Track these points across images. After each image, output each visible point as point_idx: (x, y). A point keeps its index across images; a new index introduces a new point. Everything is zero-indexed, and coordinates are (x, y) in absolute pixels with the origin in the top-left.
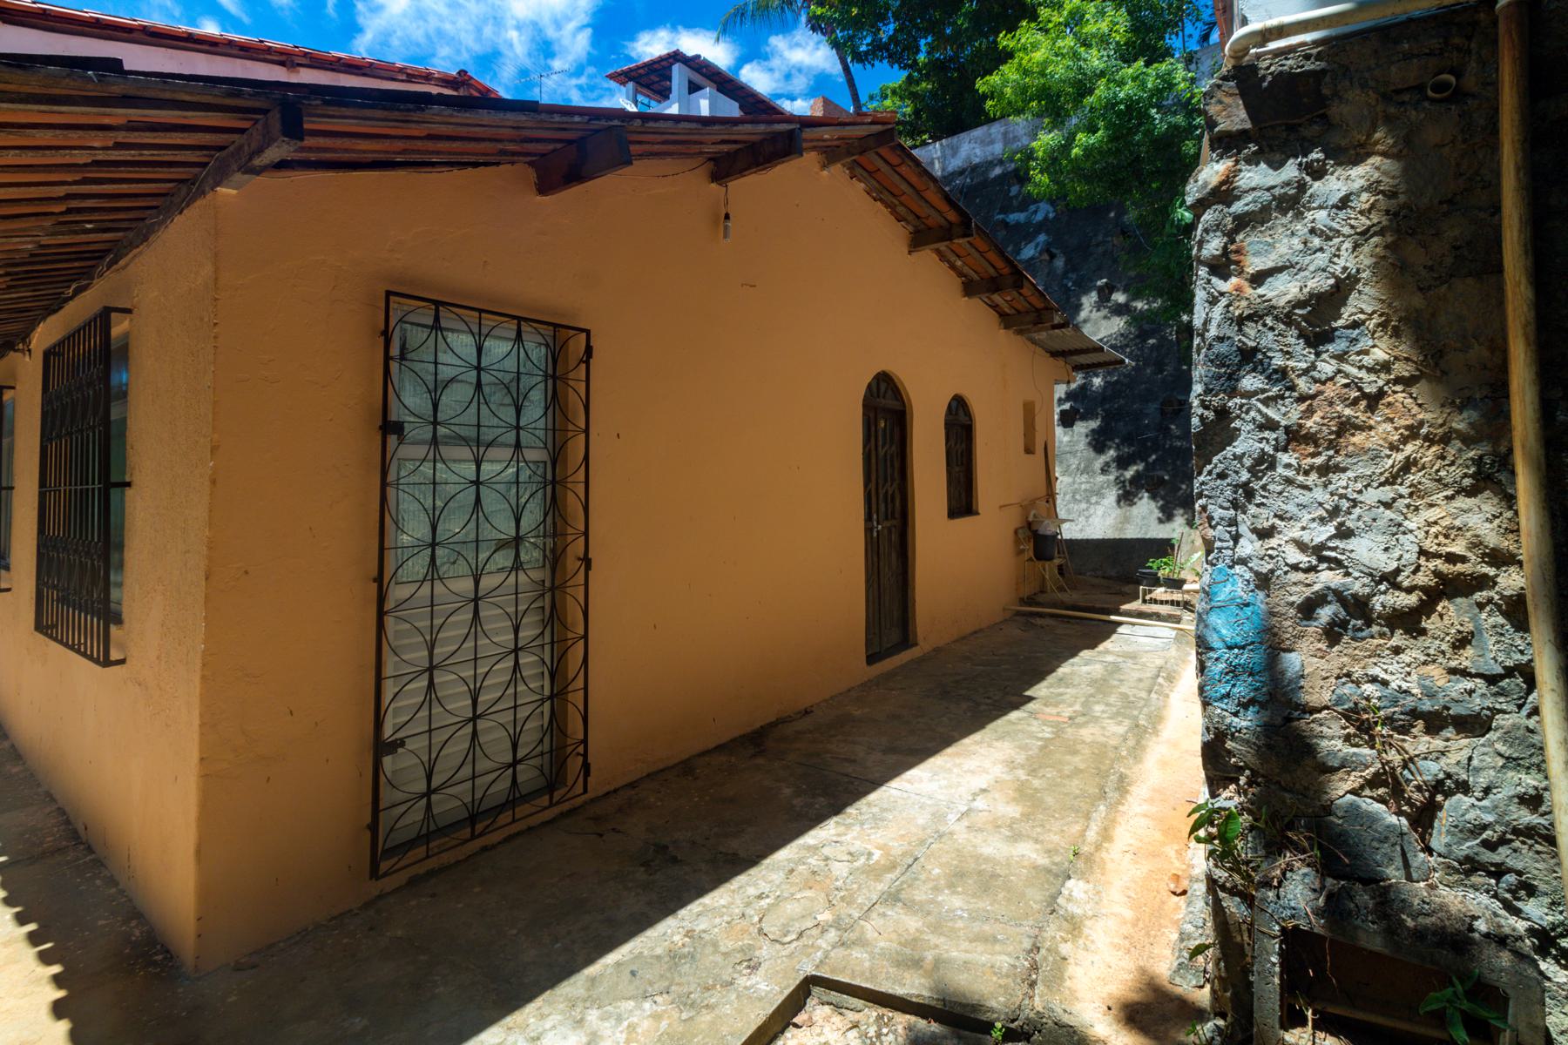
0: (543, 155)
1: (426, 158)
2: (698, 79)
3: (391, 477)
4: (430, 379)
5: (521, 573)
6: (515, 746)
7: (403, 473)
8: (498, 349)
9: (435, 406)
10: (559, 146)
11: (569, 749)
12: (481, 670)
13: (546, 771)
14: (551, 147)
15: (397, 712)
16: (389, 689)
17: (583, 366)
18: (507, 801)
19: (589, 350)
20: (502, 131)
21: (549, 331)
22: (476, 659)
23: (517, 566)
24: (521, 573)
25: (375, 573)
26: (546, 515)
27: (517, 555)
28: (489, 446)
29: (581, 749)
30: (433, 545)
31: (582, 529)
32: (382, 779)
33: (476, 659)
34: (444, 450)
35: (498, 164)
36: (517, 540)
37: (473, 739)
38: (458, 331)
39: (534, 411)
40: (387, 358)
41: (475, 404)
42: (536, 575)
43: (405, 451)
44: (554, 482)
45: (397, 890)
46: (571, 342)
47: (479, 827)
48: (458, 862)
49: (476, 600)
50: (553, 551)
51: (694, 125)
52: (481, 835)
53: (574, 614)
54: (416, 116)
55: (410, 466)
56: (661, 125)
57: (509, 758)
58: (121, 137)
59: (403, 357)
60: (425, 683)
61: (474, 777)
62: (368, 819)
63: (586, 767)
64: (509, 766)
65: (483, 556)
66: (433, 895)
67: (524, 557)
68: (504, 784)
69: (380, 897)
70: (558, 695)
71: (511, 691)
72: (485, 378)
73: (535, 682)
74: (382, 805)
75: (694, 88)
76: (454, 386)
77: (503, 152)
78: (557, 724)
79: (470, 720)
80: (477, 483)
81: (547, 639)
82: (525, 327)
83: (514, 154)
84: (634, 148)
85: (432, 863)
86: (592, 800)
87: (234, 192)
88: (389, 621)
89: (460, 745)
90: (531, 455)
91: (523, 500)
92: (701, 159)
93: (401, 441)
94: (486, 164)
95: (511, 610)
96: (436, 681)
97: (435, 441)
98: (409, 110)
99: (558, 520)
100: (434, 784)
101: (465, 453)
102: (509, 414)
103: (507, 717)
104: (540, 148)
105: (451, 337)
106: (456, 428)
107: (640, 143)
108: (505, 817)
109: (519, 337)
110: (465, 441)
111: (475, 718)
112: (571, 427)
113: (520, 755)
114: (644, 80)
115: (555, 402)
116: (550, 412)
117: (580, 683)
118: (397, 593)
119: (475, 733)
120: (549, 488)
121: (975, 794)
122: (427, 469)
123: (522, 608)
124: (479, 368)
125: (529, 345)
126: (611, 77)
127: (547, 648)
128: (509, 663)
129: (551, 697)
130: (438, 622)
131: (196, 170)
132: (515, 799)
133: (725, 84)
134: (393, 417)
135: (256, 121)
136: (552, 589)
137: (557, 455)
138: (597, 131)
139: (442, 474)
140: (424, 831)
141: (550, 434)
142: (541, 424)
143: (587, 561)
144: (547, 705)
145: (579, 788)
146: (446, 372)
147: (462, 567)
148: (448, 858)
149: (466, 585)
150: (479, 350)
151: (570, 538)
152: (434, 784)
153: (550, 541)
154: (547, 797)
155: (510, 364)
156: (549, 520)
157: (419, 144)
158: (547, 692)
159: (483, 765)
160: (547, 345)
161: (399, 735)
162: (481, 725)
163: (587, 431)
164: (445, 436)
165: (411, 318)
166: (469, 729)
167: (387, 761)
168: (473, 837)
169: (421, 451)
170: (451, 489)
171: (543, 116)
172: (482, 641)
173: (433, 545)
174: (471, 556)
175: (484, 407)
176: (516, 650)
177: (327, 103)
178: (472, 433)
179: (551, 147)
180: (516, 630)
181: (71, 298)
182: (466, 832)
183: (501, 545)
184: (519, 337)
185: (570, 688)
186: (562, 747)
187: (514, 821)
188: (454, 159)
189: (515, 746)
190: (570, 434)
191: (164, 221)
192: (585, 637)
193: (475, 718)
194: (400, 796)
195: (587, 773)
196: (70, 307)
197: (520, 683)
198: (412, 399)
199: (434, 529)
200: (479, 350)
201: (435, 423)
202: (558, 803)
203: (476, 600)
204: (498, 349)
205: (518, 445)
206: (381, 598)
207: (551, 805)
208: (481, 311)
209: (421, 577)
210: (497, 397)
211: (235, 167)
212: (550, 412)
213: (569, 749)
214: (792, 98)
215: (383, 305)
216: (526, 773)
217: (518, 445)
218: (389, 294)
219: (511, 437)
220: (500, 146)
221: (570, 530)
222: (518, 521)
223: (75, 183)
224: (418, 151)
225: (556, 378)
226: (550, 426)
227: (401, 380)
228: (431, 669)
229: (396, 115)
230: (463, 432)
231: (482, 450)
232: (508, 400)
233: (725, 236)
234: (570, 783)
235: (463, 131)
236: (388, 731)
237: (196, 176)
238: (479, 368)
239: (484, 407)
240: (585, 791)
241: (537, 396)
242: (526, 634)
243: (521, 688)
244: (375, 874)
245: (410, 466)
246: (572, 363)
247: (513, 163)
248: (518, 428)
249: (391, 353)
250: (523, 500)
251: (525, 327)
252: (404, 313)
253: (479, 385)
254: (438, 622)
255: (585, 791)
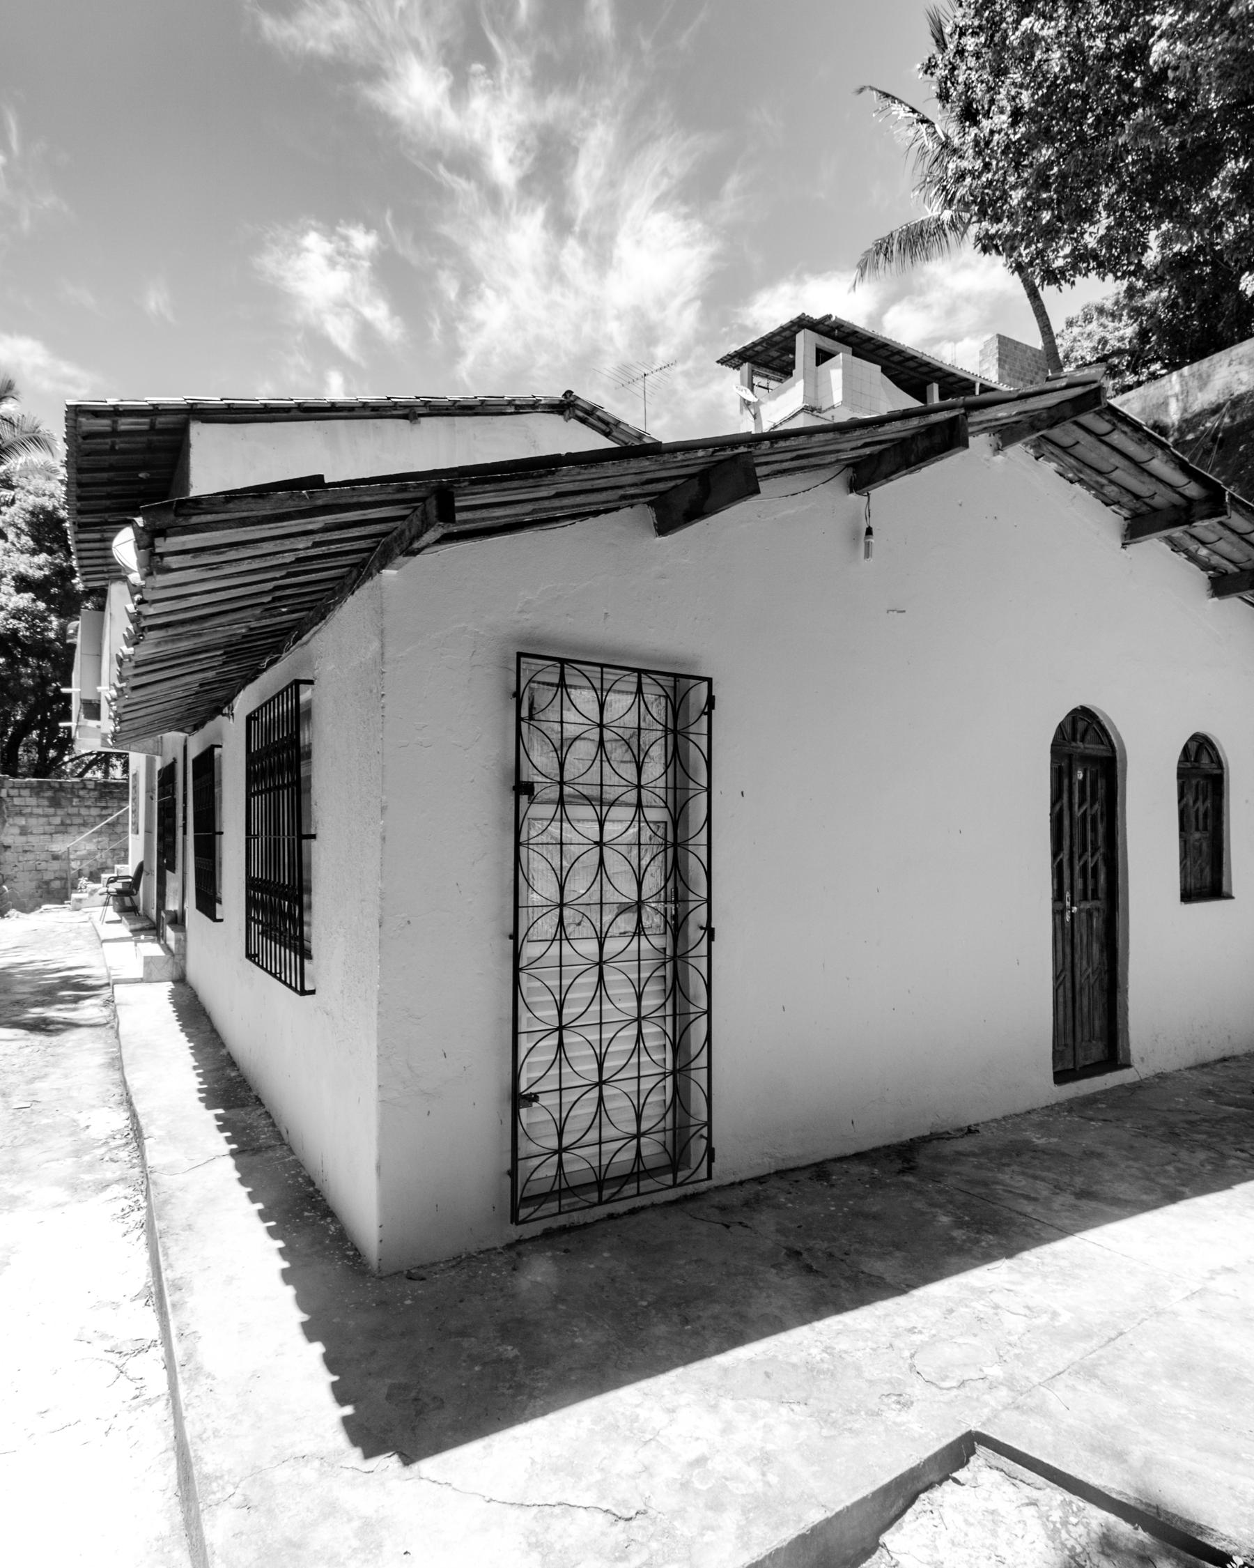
0: (662, 493)
1: (551, 514)
2: (828, 344)
3: (523, 838)
4: (556, 738)
5: (643, 938)
6: (639, 1117)
7: (533, 833)
8: (619, 704)
9: (562, 765)
10: (679, 482)
11: (693, 1130)
12: (607, 1035)
13: (669, 1147)
14: (672, 484)
15: (529, 1070)
16: (525, 1043)
17: (705, 718)
18: (632, 1173)
19: (711, 701)
20: (623, 478)
21: (668, 682)
22: (601, 1024)
23: (640, 931)
24: (643, 938)
25: (511, 930)
26: (667, 880)
27: (639, 921)
28: (612, 804)
29: (705, 1132)
30: (561, 905)
31: (705, 896)
32: (520, 1130)
33: (601, 1024)
34: (572, 811)
35: (617, 509)
36: (640, 904)
37: (599, 1105)
38: (580, 687)
39: (654, 769)
40: (519, 719)
41: (597, 762)
42: (658, 942)
43: (537, 811)
44: (675, 845)
45: (533, 1239)
46: (692, 692)
47: (606, 1193)
48: (586, 1225)
49: (601, 963)
50: (675, 917)
51: (830, 436)
52: (607, 1202)
53: (696, 986)
54: (547, 480)
55: (539, 826)
56: (792, 442)
57: (633, 1129)
58: (318, 538)
59: (531, 717)
60: (556, 1042)
61: (600, 1143)
62: (508, 1166)
63: (710, 1151)
64: (634, 1137)
65: (607, 918)
66: (566, 1251)
67: (646, 923)
68: (628, 1155)
69: (520, 1241)
70: (680, 1072)
71: (634, 1060)
72: (608, 735)
73: (658, 1056)
74: (521, 1154)
75: (823, 356)
76: (577, 743)
77: (624, 497)
78: (679, 1101)
79: (596, 1084)
80: (600, 844)
81: (669, 1011)
82: (645, 680)
83: (633, 496)
84: (760, 471)
85: (562, 1220)
86: (717, 1188)
87: (394, 572)
88: (523, 977)
89: (586, 1109)
90: (653, 814)
91: (644, 863)
92: (837, 468)
93: (531, 803)
94: (607, 511)
95: (634, 976)
96: (565, 1041)
97: (561, 802)
98: (540, 476)
99: (680, 886)
100: (566, 1142)
101: (588, 812)
102: (629, 772)
103: (631, 1087)
104: (661, 487)
105: (572, 692)
106: (576, 787)
107: (767, 463)
108: (630, 1189)
109: (639, 691)
110: (588, 800)
111: (600, 1083)
112: (692, 785)
113: (644, 1127)
114: (763, 357)
115: (676, 759)
116: (670, 770)
117: (703, 1061)
118: (530, 951)
119: (601, 1099)
120: (670, 851)
121: (1212, 1271)
122: (554, 829)
123: (645, 975)
124: (601, 726)
125: (649, 698)
126: (722, 361)
127: (669, 1020)
128: (632, 1031)
129: (674, 1072)
130: (566, 982)
131: (365, 555)
132: (639, 1172)
133: (865, 346)
134: (524, 778)
135: (415, 509)
136: (675, 958)
137: (678, 815)
138: (720, 462)
139: (569, 835)
140: (556, 1187)
141: (670, 792)
142: (661, 782)
143: (710, 932)
144: (669, 1080)
145: (703, 1173)
146: (570, 731)
147: (587, 930)
148: (577, 1218)
149: (591, 948)
150: (602, 706)
151: (692, 905)
152: (566, 1142)
153: (671, 907)
154: (670, 1176)
155: (631, 720)
156: (670, 885)
157: (546, 504)
158: (669, 1066)
159: (609, 1132)
160: (667, 697)
161: (533, 1090)
162: (607, 1091)
163: (709, 789)
164: (569, 796)
165: (539, 678)
166: (595, 1093)
167: (523, 1112)
168: (601, 1202)
169: (549, 810)
170: (576, 850)
171: (667, 457)
172: (607, 1006)
173: (561, 905)
174: (595, 917)
175: (606, 764)
176: (639, 1019)
177: (473, 483)
178: (595, 792)
179: (672, 484)
180: (639, 998)
181: (265, 670)
182: (594, 1197)
183: (623, 909)
184: (639, 691)
185: (693, 1065)
186: (685, 1128)
187: (638, 1194)
188: (576, 511)
189: (639, 1117)
190: (691, 793)
191: (339, 602)
192: (709, 1012)
193: (600, 1083)
194: (534, 1149)
195: (711, 1159)
196: (264, 678)
197: (643, 1053)
198: (541, 758)
199: (562, 888)
200: (602, 706)
201: (562, 783)
202: (681, 1184)
203: (601, 963)
204: (619, 704)
205: (639, 806)
206: (517, 955)
207: (675, 1185)
208: (602, 666)
209: (550, 937)
210: (617, 752)
211: (397, 551)
212: (670, 770)
213: (693, 1130)
214: (955, 339)
215: (514, 666)
216: (650, 1147)
217: (639, 806)
218: (520, 655)
219: (632, 797)
220: (621, 492)
221: (692, 897)
222: (640, 884)
223: (282, 578)
224: (546, 510)
225: (676, 733)
226: (670, 784)
227: (530, 740)
228: (560, 1028)
229: (530, 482)
230: (586, 791)
231: (605, 809)
232: (628, 757)
233: (867, 555)
234: (694, 1165)
235: (587, 485)
236: (523, 1086)
237: (365, 561)
238: (601, 726)
239: (606, 764)
240: (710, 1177)
241: (657, 752)
242: (650, 1002)
243: (644, 1058)
244: (515, 1219)
245: (539, 826)
246: (693, 715)
247: (632, 506)
248: (639, 787)
249: (524, 711)
250: (644, 863)
251: (645, 680)
252: (537, 674)
253: (601, 743)
254: (566, 982)
255: (710, 1177)
